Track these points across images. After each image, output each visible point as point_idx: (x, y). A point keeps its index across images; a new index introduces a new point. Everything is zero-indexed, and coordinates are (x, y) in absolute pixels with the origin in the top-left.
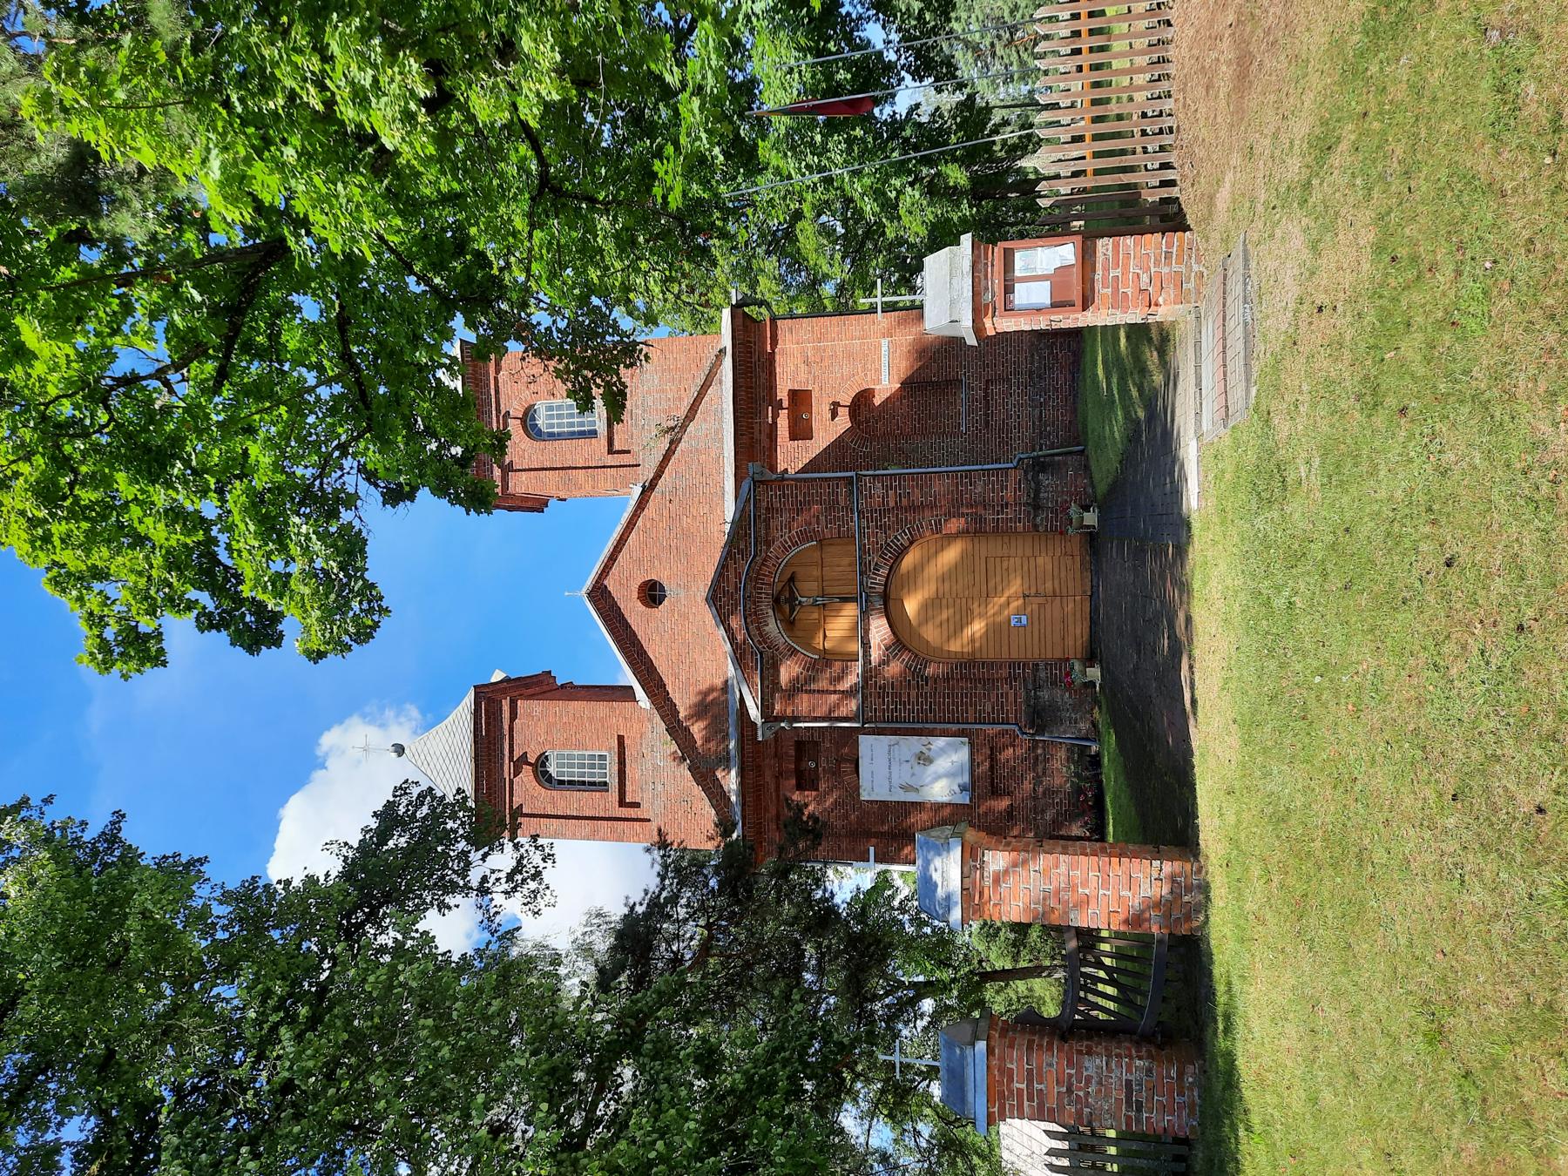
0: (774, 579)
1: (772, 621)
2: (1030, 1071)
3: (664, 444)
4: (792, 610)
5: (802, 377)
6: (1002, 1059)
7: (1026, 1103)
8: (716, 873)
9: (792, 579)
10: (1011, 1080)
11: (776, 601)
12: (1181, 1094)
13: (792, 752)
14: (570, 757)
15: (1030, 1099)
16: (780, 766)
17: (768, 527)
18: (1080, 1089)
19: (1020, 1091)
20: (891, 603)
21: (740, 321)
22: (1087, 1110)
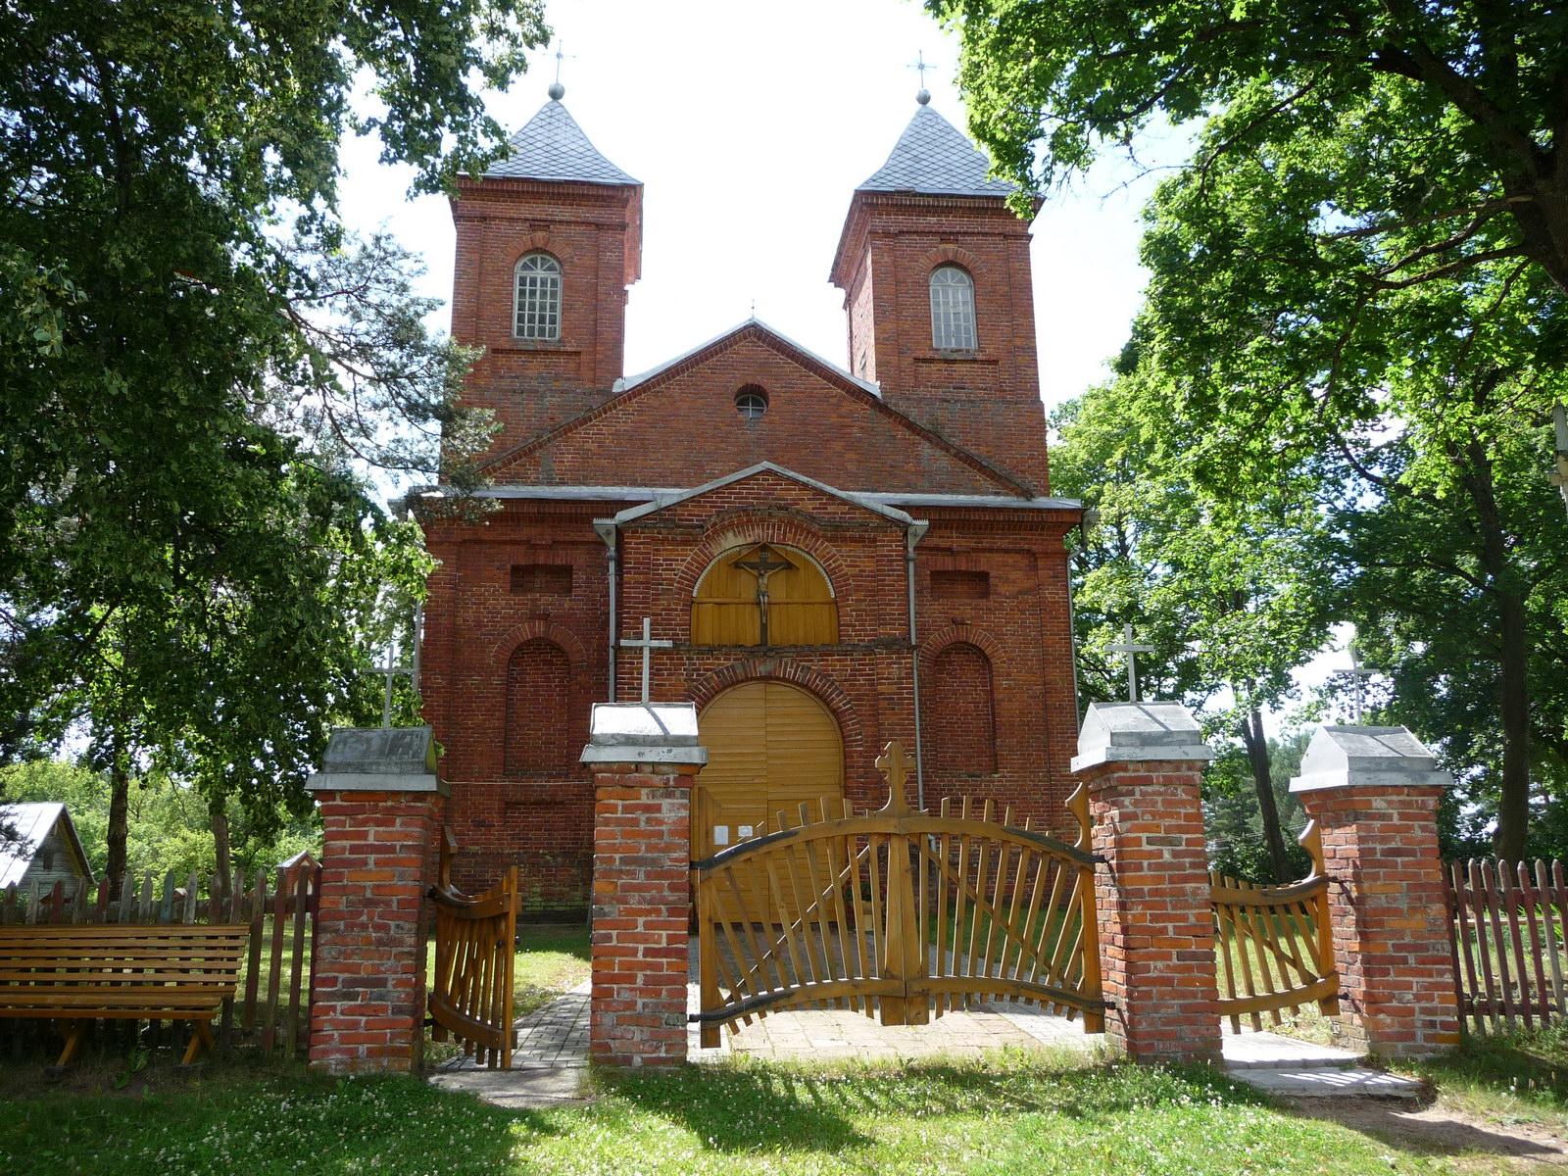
0: (793, 547)
1: (741, 541)
2: (391, 849)
3: (923, 423)
4: (753, 566)
5: (1003, 589)
6: (409, 812)
7: (347, 843)
8: (1491, 462)
9: (789, 566)
10: (378, 823)
11: (764, 547)
12: (371, 1053)
13: (558, 562)
14: (554, 295)
15: (354, 849)
16: (543, 547)
17: (853, 540)
18: (371, 918)
19: (364, 835)
20: (761, 686)
21: (1067, 518)
22: (341, 925)
